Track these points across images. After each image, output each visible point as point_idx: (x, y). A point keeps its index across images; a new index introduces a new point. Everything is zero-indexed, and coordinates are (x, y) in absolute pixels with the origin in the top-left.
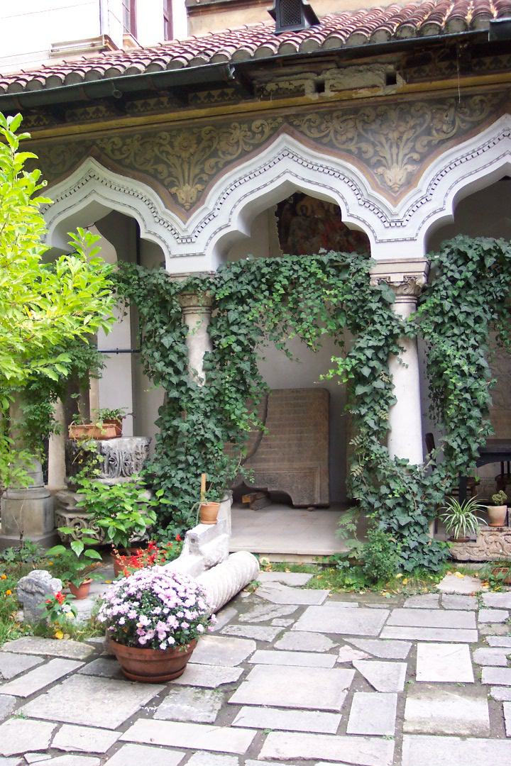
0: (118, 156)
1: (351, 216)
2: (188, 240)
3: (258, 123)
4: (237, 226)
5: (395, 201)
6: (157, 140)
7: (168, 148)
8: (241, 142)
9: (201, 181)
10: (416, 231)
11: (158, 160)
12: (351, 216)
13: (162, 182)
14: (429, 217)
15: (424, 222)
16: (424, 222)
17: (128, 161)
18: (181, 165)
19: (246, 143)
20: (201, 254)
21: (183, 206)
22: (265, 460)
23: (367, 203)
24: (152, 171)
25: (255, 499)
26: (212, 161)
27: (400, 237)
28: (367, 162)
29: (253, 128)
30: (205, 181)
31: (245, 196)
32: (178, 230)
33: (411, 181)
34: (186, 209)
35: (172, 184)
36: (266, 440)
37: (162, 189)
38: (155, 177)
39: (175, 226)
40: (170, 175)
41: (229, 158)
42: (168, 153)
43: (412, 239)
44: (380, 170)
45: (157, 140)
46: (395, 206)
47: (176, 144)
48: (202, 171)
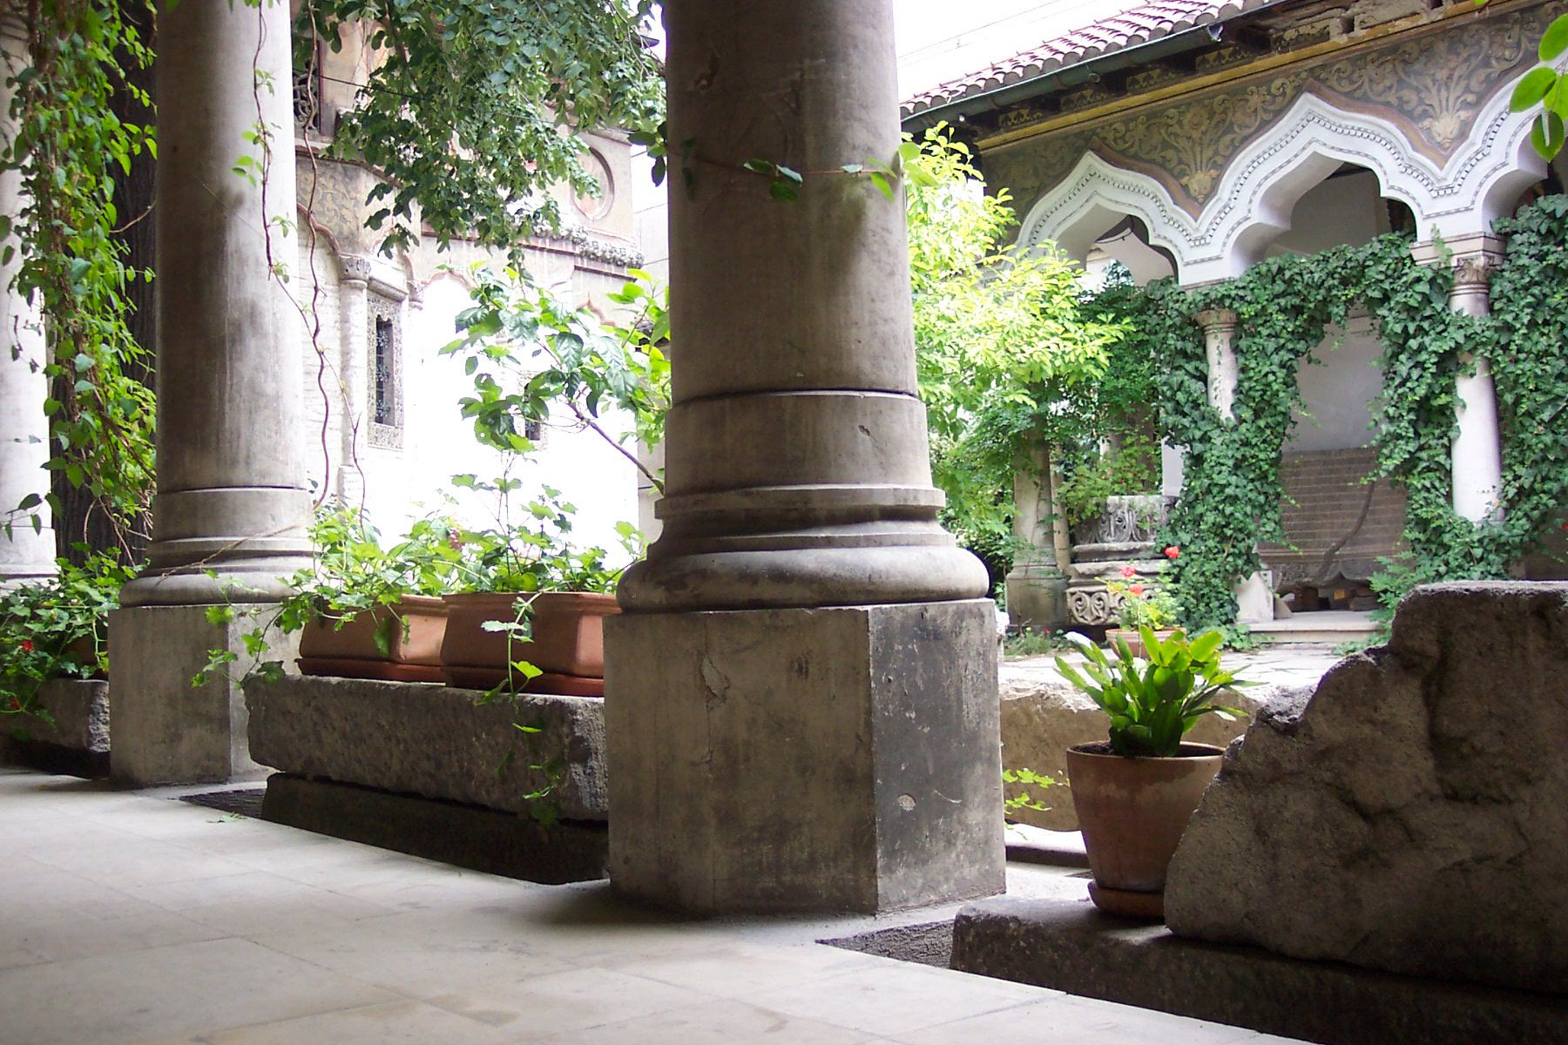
0: (1122, 146)
1: (1392, 187)
2: (1201, 241)
3: (1278, 82)
4: (1260, 216)
5: (1442, 161)
6: (1164, 120)
7: (1176, 129)
8: (1260, 111)
9: (1216, 166)
10: (1471, 197)
11: (1166, 145)
12: (1392, 187)
13: (1171, 172)
14: (1487, 176)
15: (1481, 184)
16: (1481, 184)
17: (1132, 151)
18: (1192, 148)
19: (1265, 111)
20: (1218, 258)
21: (1196, 199)
22: (1371, 541)
23: (1409, 168)
24: (1159, 160)
25: (1353, 594)
26: (1228, 138)
27: (1452, 208)
28: (1410, 115)
29: (1273, 91)
30: (1219, 166)
31: (1266, 178)
32: (1190, 230)
33: (1463, 135)
34: (1195, 202)
35: (1183, 174)
36: (1373, 512)
37: (1170, 180)
38: (1162, 166)
39: (1186, 226)
40: (1180, 162)
41: (1246, 132)
42: (1176, 135)
43: (1467, 209)
44: (1426, 123)
45: (1164, 120)
46: (1441, 168)
47: (1185, 122)
48: (1216, 153)
